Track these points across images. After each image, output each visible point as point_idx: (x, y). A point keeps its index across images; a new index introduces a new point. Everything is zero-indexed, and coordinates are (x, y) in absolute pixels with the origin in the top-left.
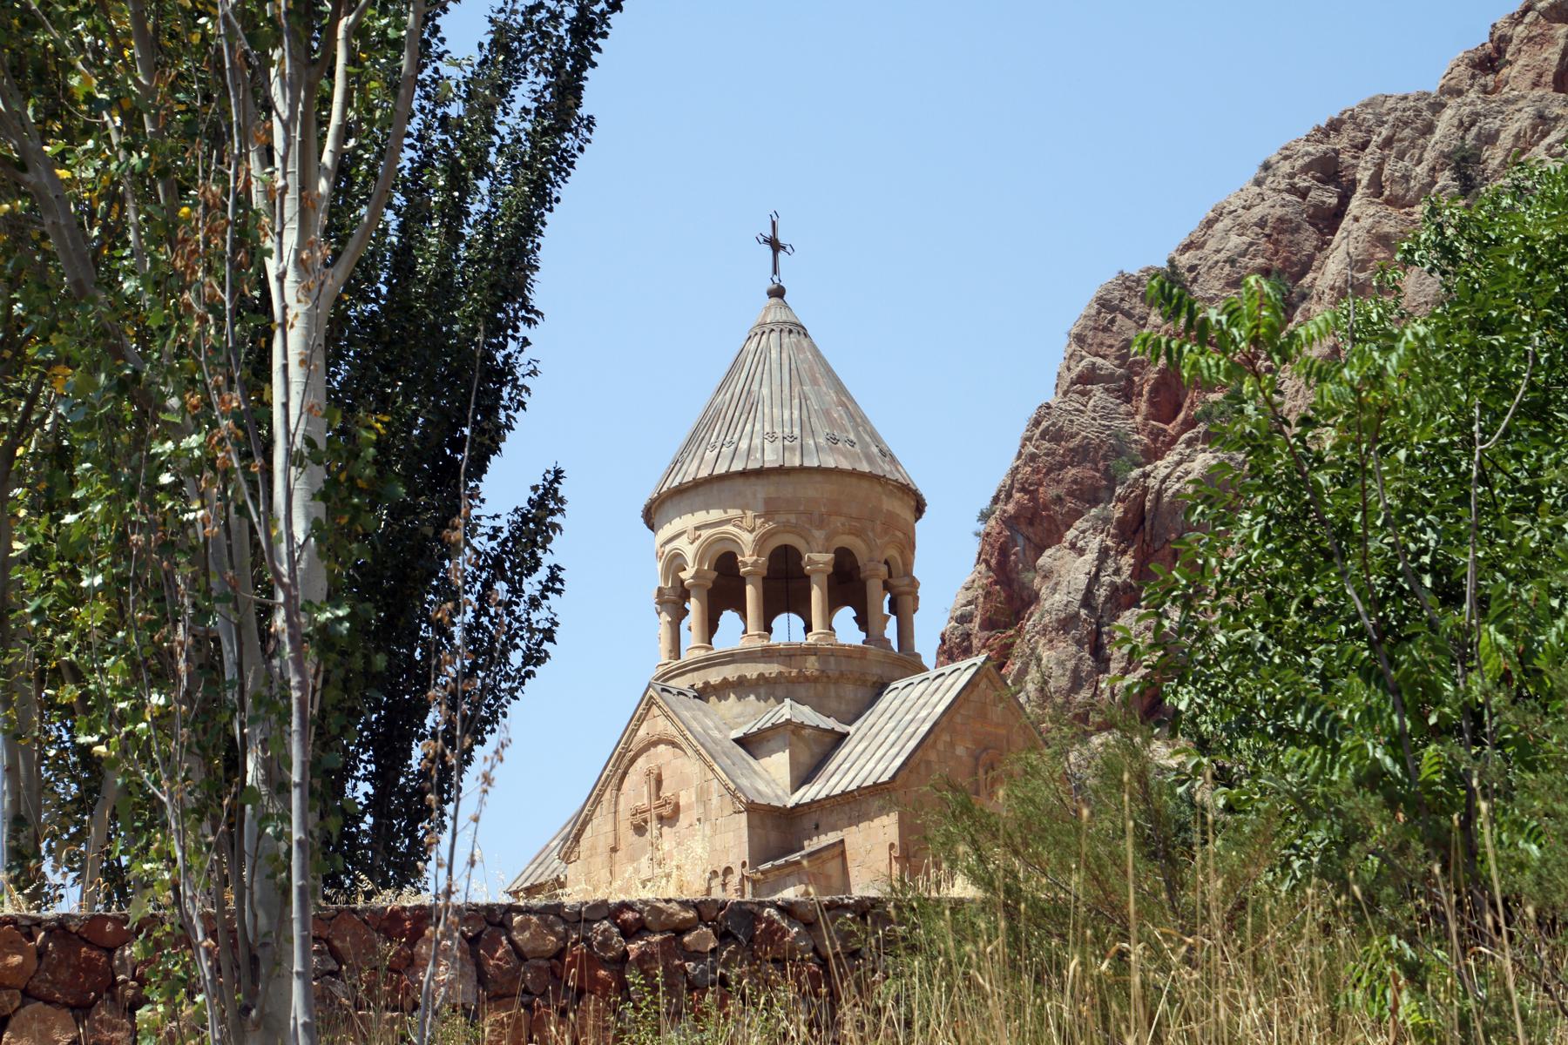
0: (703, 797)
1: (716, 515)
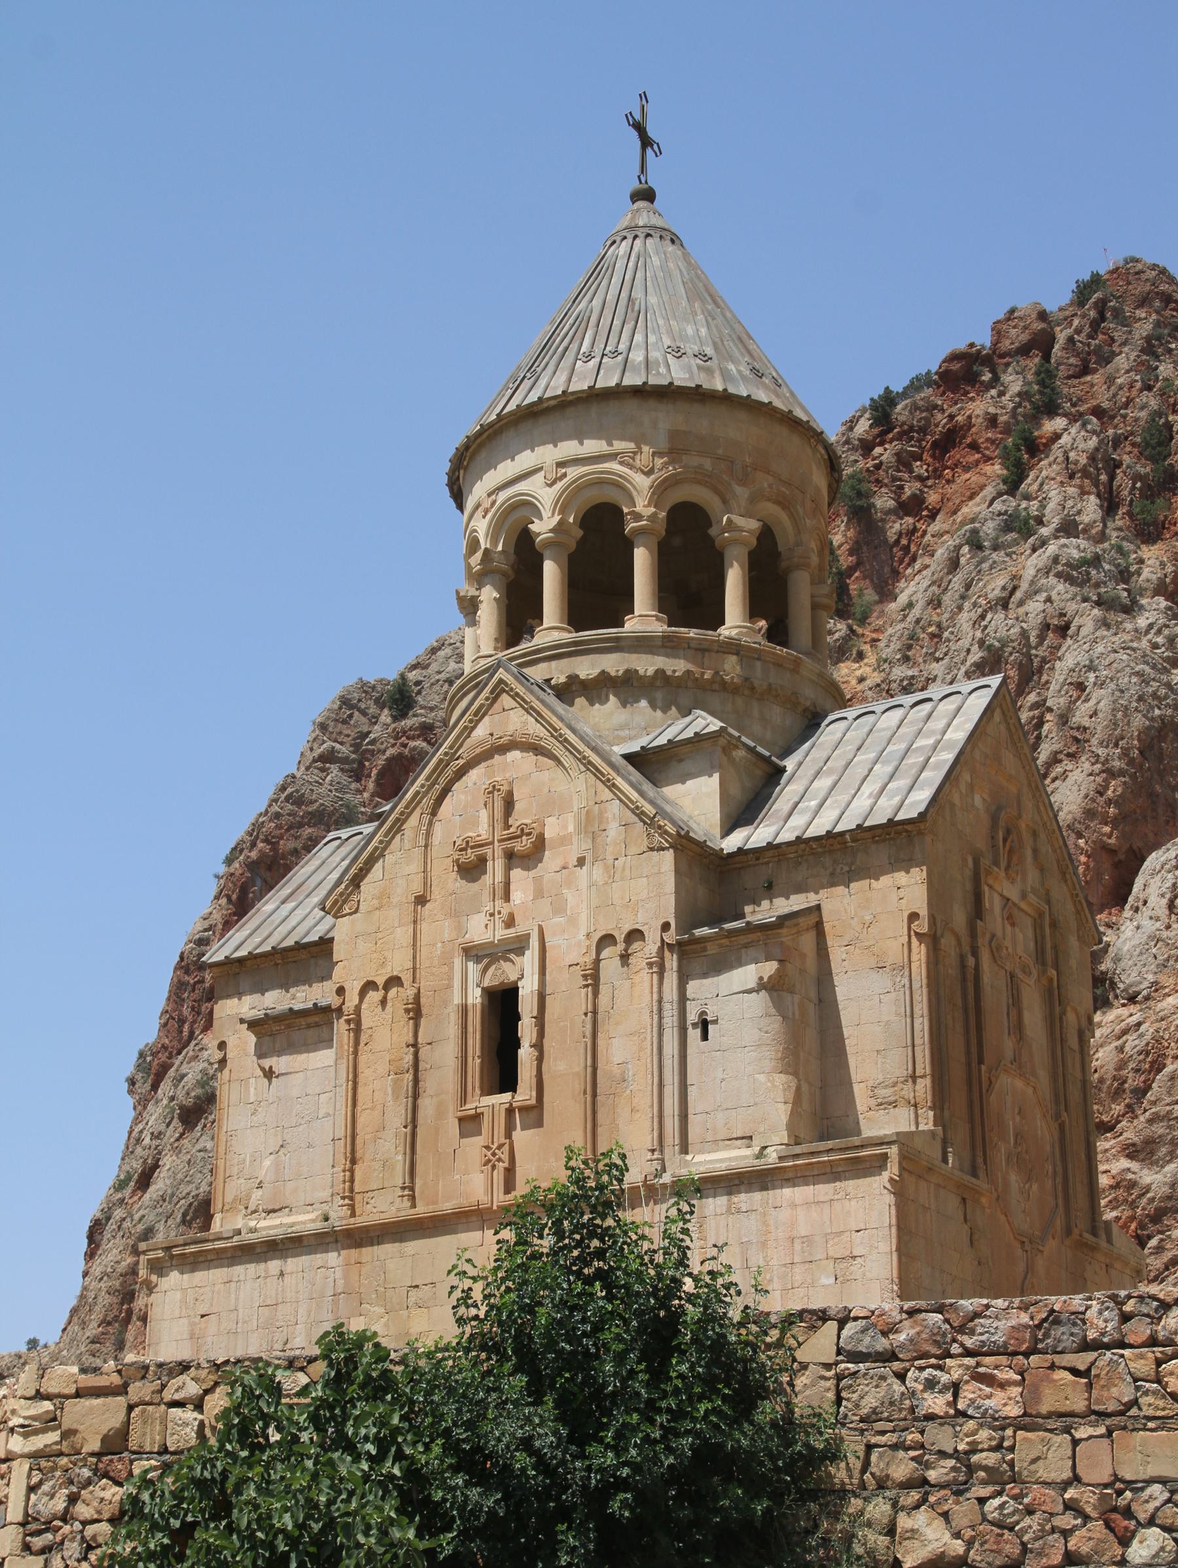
0: (591, 826)
1: (593, 446)
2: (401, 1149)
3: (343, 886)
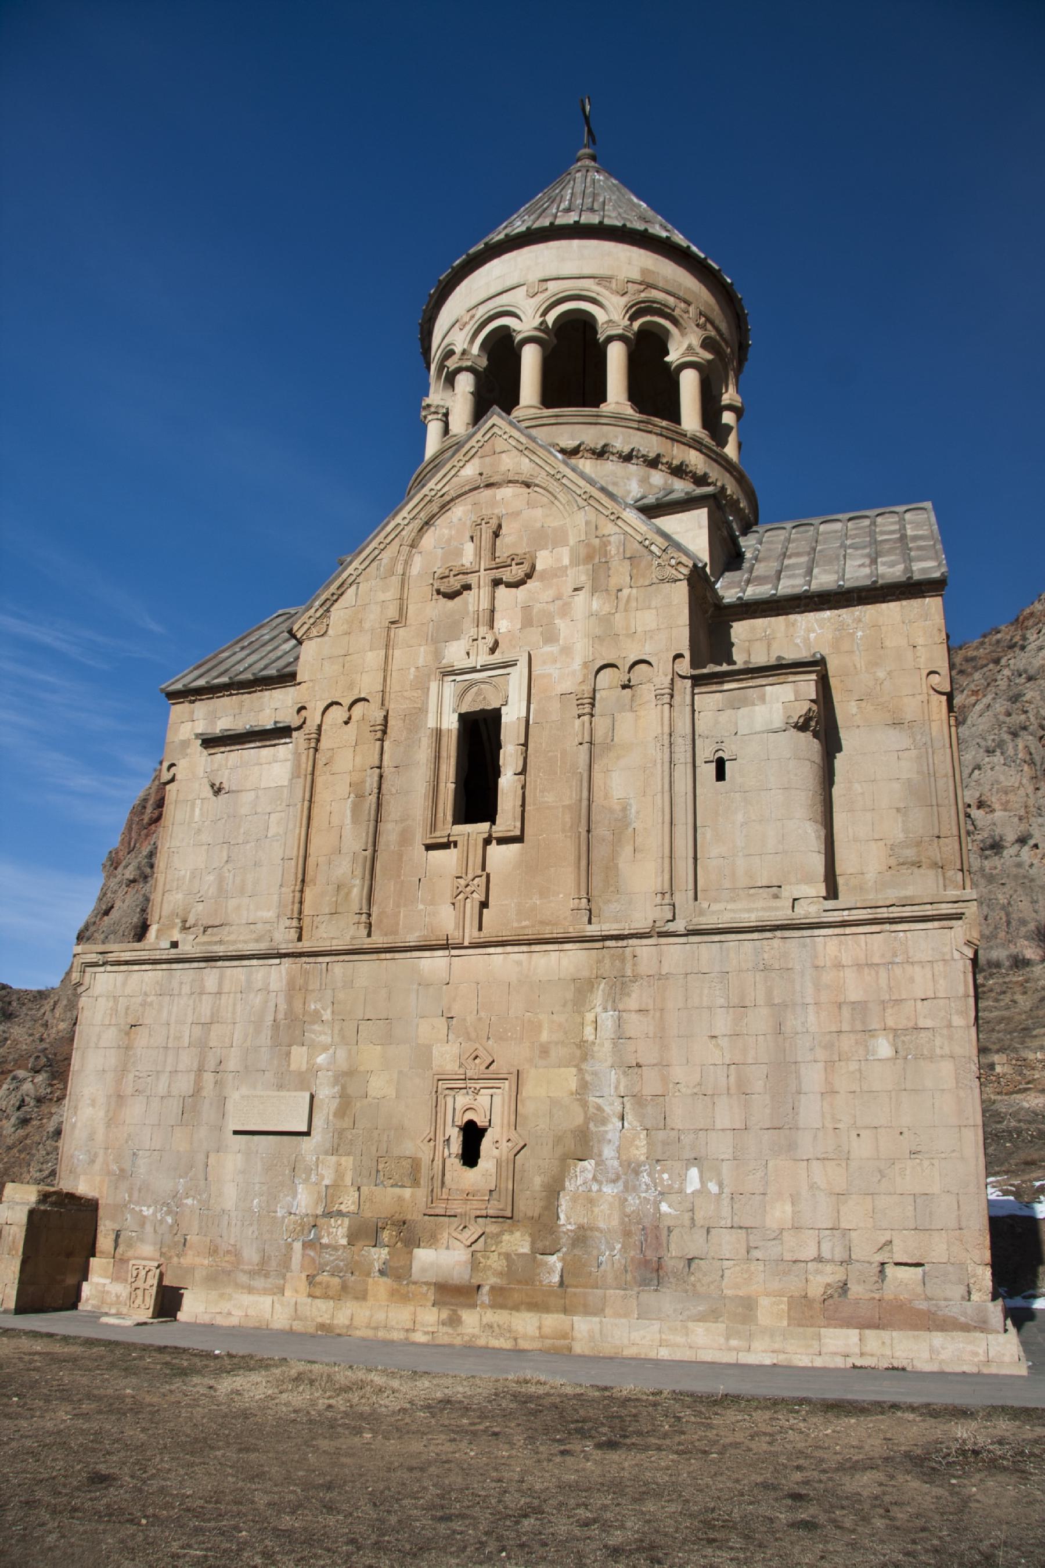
2: (358, 872)
3: (313, 610)
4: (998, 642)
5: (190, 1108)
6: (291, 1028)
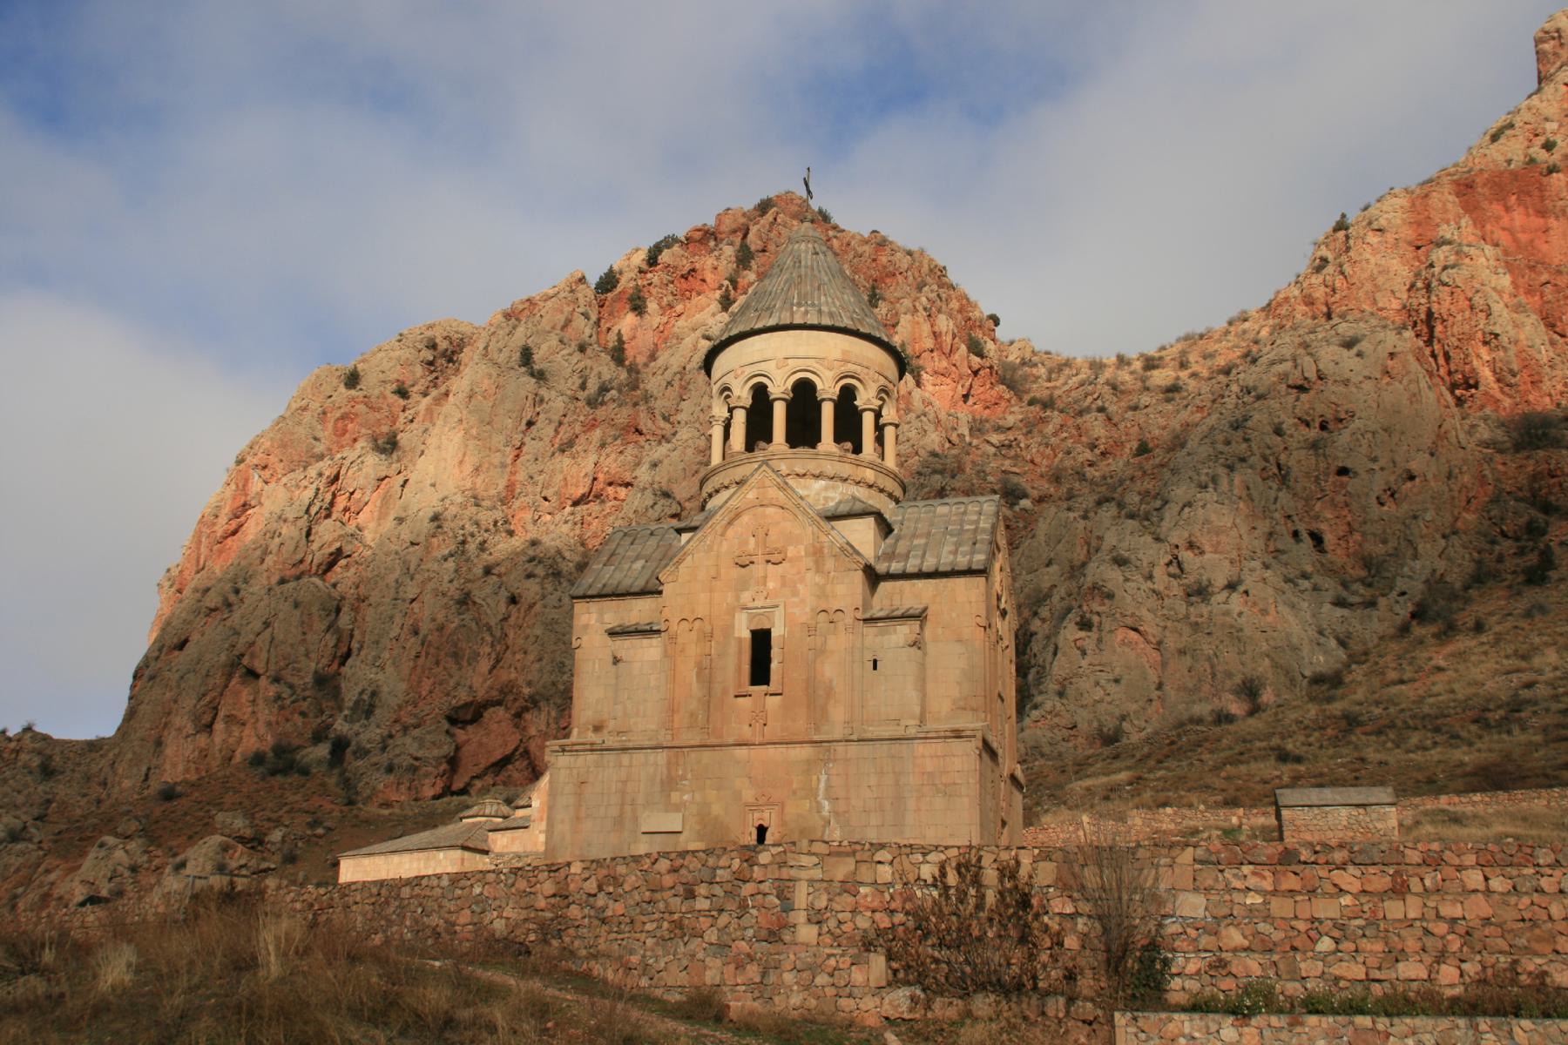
0: (817, 553)
4: (1244, 332)
5: (619, 822)
6: (670, 783)
